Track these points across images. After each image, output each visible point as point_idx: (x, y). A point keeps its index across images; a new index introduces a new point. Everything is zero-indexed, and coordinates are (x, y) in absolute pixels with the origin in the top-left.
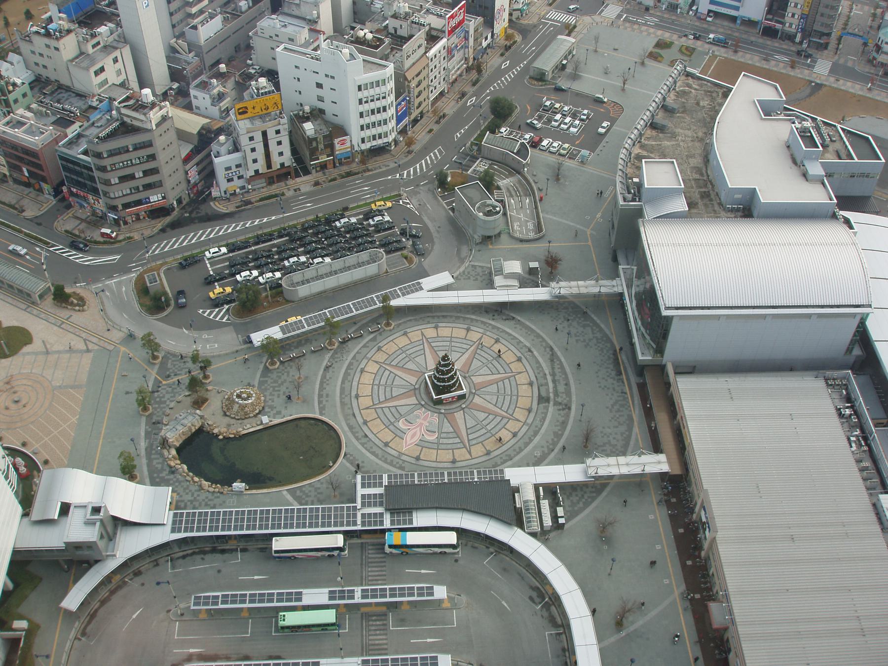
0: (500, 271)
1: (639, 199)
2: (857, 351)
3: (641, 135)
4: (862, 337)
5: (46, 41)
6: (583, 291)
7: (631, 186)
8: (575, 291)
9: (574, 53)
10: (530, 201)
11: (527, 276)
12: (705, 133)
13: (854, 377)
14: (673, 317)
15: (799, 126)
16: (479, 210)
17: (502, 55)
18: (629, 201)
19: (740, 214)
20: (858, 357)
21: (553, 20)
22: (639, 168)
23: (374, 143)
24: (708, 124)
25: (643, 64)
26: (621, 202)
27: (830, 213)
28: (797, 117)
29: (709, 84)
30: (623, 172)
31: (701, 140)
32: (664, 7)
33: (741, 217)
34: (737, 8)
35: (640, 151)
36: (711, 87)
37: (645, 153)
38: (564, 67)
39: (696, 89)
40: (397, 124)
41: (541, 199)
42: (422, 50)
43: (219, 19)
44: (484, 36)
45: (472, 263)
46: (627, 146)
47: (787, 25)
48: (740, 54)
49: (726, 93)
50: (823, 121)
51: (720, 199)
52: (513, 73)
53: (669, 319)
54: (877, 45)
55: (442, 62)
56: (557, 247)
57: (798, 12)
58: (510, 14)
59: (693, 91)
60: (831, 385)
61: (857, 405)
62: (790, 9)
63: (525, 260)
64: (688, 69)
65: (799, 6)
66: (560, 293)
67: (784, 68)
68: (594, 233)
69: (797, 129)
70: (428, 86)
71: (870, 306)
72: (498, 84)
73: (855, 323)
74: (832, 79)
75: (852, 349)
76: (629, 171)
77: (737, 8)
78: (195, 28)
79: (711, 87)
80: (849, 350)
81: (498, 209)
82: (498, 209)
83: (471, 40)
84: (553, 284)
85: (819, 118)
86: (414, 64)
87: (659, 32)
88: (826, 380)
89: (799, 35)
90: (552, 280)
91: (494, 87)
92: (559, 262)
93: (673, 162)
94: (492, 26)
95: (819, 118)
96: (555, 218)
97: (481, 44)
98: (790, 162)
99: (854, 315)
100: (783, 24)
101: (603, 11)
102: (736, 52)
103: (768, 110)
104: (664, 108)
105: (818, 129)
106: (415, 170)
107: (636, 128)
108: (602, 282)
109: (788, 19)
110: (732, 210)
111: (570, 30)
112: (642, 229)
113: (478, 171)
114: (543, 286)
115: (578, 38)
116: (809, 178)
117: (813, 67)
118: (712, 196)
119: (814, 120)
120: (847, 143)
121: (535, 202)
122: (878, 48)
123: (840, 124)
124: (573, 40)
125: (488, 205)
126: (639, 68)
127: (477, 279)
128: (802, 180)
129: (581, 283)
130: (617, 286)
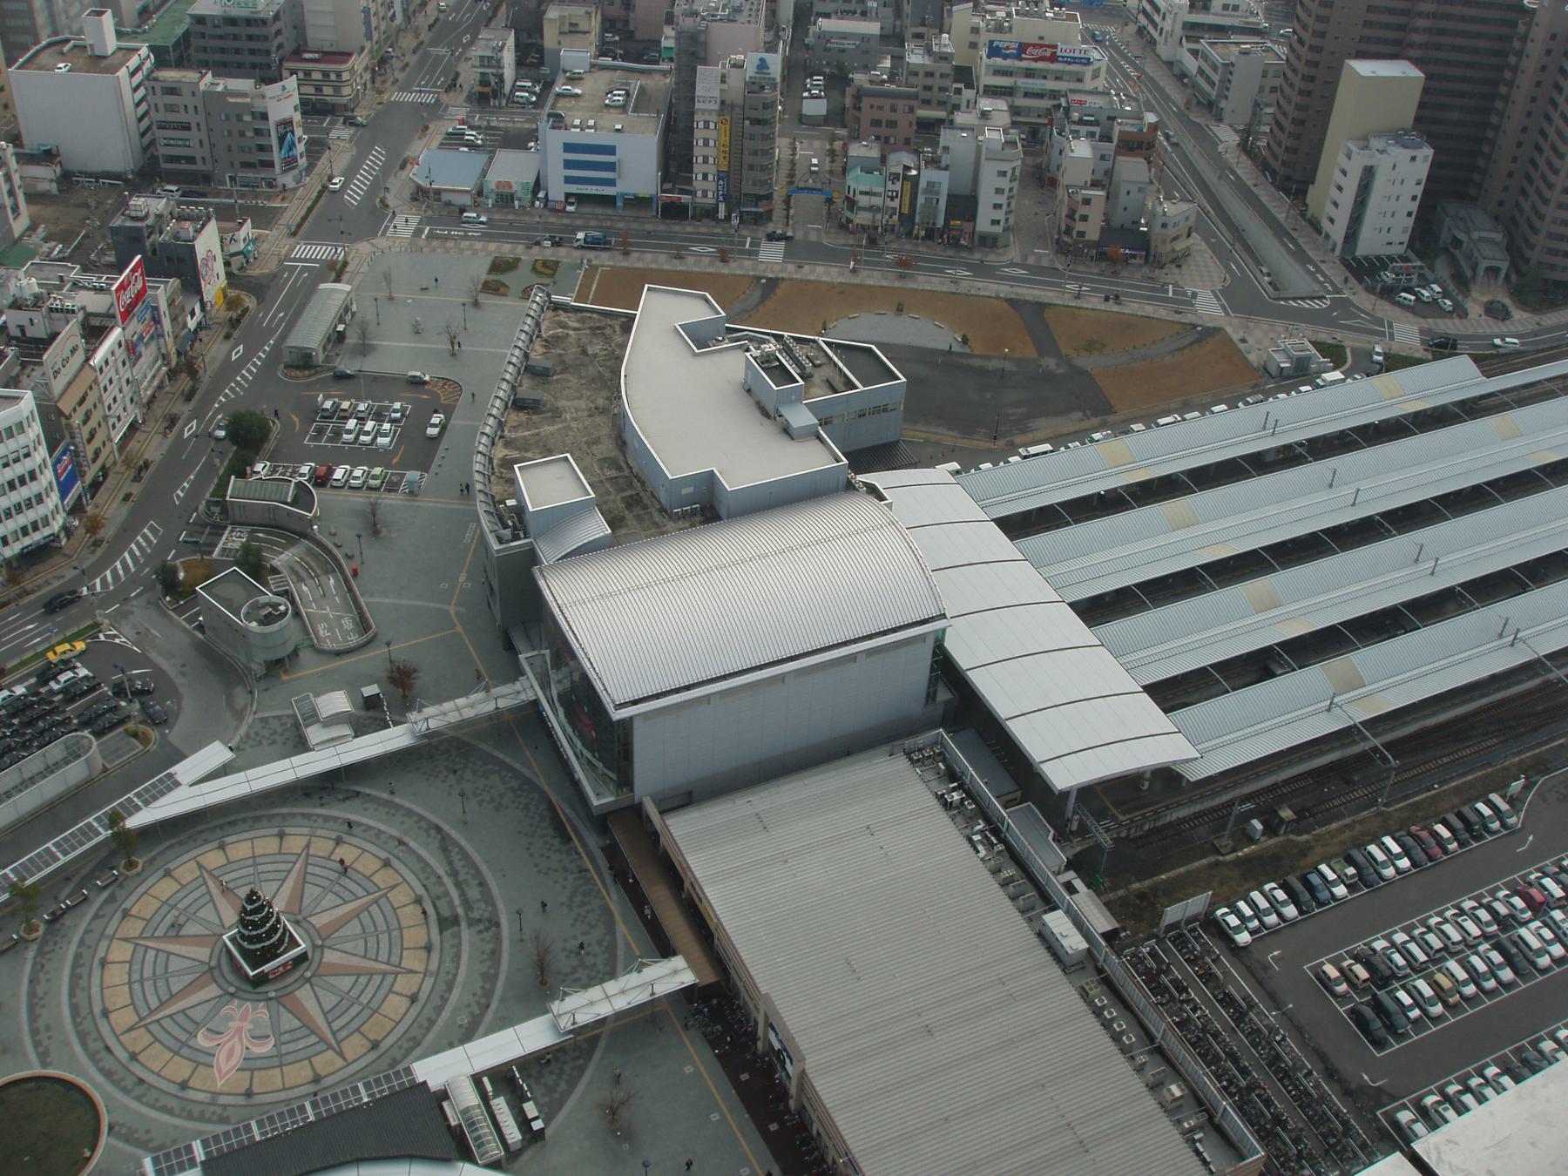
0: (313, 717)
1: (525, 534)
2: (944, 695)
3: (501, 425)
4: (945, 669)
6: (469, 713)
7: (506, 515)
8: (454, 718)
9: (354, 308)
10: (337, 580)
11: (363, 713)
12: (608, 398)
13: (951, 738)
14: (631, 718)
15: (757, 353)
16: (249, 617)
17: (227, 337)
18: (508, 542)
19: (698, 519)
20: (946, 703)
21: (305, 260)
22: (512, 481)
23: (27, 541)
24: (609, 382)
25: (476, 304)
26: (496, 546)
27: (842, 482)
28: (751, 339)
29: (595, 316)
30: (486, 494)
31: (604, 411)
32: (490, 202)
33: (702, 523)
34: (612, 183)
35: (506, 452)
37: (515, 454)
38: (341, 337)
39: (575, 329)
40: (63, 498)
41: (355, 573)
42: (80, 356)
44: (188, 310)
45: (260, 715)
46: (481, 448)
47: (699, 194)
48: (634, 256)
51: (660, 502)
52: (255, 365)
53: (627, 724)
54: (847, 198)
56: (403, 648)
57: (711, 170)
58: (227, 264)
59: (571, 332)
60: (918, 760)
61: (968, 781)
62: (698, 168)
63: (352, 687)
64: (554, 298)
65: (711, 160)
66: (428, 728)
67: (711, 264)
68: (462, 609)
69: (755, 359)
70: (106, 418)
71: (943, 616)
72: (232, 389)
73: (925, 654)
74: (791, 267)
75: (935, 692)
76: (496, 489)
77: (612, 183)
79: (600, 321)
80: (931, 696)
81: (282, 608)
82: (282, 608)
83: (166, 323)
84: (413, 716)
85: (786, 334)
86: (70, 383)
87: (492, 246)
88: (908, 754)
89: (722, 207)
90: (410, 709)
91: (226, 396)
92: (414, 675)
93: (566, 459)
94: (199, 292)
96: (387, 601)
97: (185, 325)
98: (758, 414)
99: (923, 637)
100: (692, 193)
102: (626, 253)
103: (701, 337)
104: (530, 370)
105: (788, 351)
106: (115, 573)
107: (490, 415)
108: (495, 691)
109: (698, 183)
110: (684, 516)
111: (337, 271)
112: (542, 583)
113: (231, 550)
114: (396, 724)
115: (356, 283)
116: (793, 433)
117: (757, 253)
118: (646, 501)
119: (778, 338)
121: (346, 581)
122: (851, 203)
124: (347, 288)
125: (264, 606)
127: (274, 742)
128: (785, 440)
129: (461, 701)
130: (526, 689)
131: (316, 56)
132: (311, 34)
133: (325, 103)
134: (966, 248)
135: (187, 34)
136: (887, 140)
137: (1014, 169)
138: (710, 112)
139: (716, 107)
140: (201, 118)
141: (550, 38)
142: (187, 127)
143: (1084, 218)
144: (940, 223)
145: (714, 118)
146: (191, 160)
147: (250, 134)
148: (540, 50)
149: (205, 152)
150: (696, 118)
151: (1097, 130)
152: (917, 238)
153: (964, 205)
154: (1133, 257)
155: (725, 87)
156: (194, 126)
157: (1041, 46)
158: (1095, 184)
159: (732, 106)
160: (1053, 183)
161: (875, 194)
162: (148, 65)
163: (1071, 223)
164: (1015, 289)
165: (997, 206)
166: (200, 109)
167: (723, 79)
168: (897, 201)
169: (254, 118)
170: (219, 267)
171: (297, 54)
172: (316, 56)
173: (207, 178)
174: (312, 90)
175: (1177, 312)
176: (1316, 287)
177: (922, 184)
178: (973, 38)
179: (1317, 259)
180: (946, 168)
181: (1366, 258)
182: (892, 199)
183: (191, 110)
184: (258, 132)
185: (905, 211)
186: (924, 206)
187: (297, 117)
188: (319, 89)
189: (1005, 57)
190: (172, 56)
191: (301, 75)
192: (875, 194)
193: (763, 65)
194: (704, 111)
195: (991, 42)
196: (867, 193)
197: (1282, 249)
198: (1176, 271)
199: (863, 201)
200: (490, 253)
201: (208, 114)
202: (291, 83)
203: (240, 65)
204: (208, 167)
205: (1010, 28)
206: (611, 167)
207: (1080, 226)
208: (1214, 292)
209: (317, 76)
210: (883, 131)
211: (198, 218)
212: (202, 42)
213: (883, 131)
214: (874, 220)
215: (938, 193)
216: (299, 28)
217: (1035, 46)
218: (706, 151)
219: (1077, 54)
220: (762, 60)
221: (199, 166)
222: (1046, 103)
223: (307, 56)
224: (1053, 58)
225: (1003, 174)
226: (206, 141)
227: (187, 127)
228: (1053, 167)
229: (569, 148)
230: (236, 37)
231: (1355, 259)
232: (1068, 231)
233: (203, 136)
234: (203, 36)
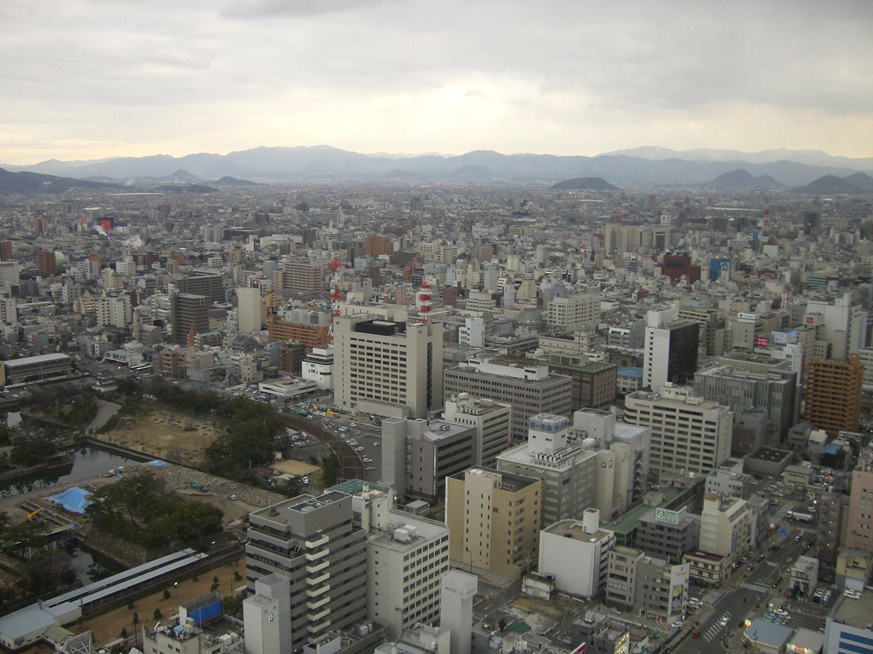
5: (170, 641)
43: (338, 640)
78: (313, 646)
131: (703, 554)
135: (636, 530)
140: (633, 576)
141: (841, 567)
142: (624, 579)
146: (623, 597)
147: (658, 590)
148: (833, 574)
149: (632, 595)
156: (629, 580)
162: (612, 542)
166: (634, 571)
171: (693, 551)
172: (703, 554)
173: (629, 609)
174: (697, 573)
183: (629, 570)
184: (663, 590)
187: (686, 586)
188: (700, 573)
190: (625, 540)
191: (692, 563)
202: (686, 566)
203: (660, 552)
204: (631, 603)
209: (701, 565)
211: (621, 630)
212: (643, 536)
216: (696, 537)
221: (627, 602)
223: (698, 553)
226: (633, 589)
227: (624, 579)
230: (661, 536)
234: (644, 532)
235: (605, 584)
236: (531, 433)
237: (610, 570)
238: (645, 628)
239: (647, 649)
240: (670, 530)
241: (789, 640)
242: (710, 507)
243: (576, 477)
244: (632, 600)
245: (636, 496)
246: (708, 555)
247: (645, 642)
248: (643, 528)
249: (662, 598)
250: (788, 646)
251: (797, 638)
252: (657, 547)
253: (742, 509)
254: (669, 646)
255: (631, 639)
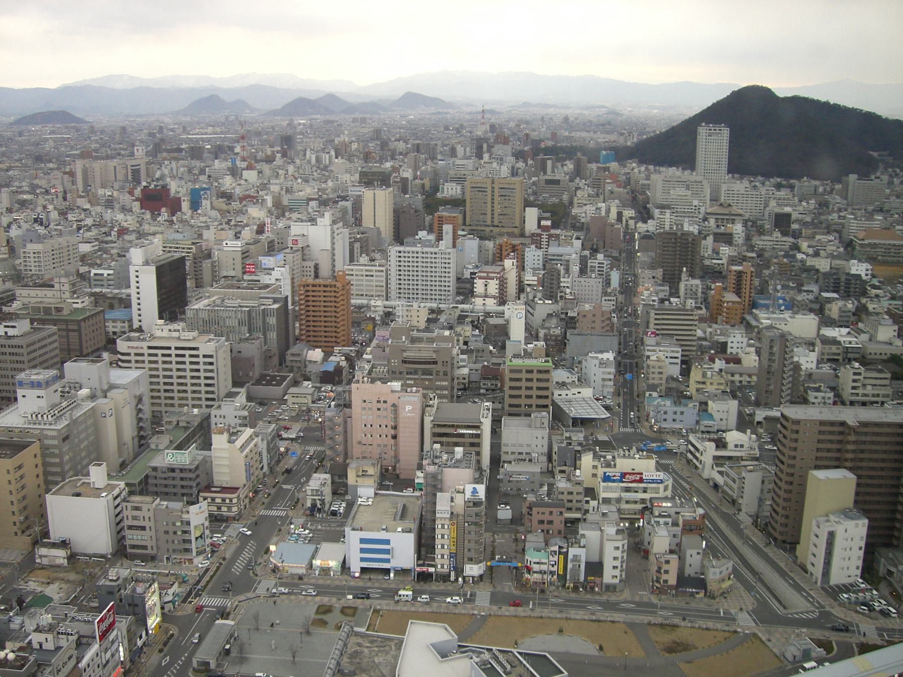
15: (477, 660)
17: (161, 651)
25: (308, 633)
28: (473, 652)
29: (379, 639)
32: (317, 573)
34: (388, 561)
36: (382, 642)
38: (228, 652)
39: (367, 647)
42: (73, 661)
47: (439, 566)
49: (399, 644)
50: (499, 650)
52: (175, 668)
54: (527, 567)
55: (97, 670)
57: (446, 552)
58: (162, 608)
59: (366, 650)
62: (438, 551)
64: (356, 629)
65: (446, 547)
69: (477, 663)
74: (495, 608)
77: (388, 561)
79: (382, 642)
89: (453, 574)
95: (494, 648)
97: (136, 644)
101: (256, 588)
103: (444, 653)
105: (496, 658)
109: (439, 561)
115: (237, 620)
117: (474, 601)
119: (489, 650)
120: (528, 666)
122: (529, 570)
123: (516, 648)
124: (232, 623)
126: (307, 639)
131: (219, 489)
132: (216, 478)
133: (222, 516)
134: (598, 593)
135: (147, 477)
136: (548, 531)
137: (623, 545)
138: (445, 519)
139: (449, 516)
140: (152, 524)
141: (351, 478)
142: (143, 528)
143: (666, 572)
144: (582, 578)
145: (447, 522)
146: (145, 548)
147: (179, 533)
148: (346, 485)
149: (154, 543)
150: (437, 522)
151: (669, 520)
152: (568, 588)
153: (595, 568)
154: (698, 593)
155: (453, 504)
156: (148, 528)
157: (634, 474)
158: (671, 552)
159: (458, 515)
160: (646, 553)
161: (542, 563)
162: (124, 493)
163: (659, 575)
164: (630, 616)
165: (615, 567)
166: (152, 519)
167: (452, 500)
168: (556, 567)
169: (182, 524)
170: (158, 609)
171: (208, 488)
172: (219, 489)
173: (153, 558)
174: (215, 509)
175: (728, 626)
176: (809, 605)
177: (570, 556)
178: (594, 471)
179: (807, 589)
180: (584, 547)
181: (837, 586)
182: (553, 566)
184: (185, 532)
185: (561, 572)
186: (571, 570)
187: (207, 524)
188: (219, 508)
189: (614, 481)
190: (138, 489)
191: (209, 500)
192: (542, 563)
193: (475, 491)
194: (441, 518)
195: (605, 473)
196: (538, 563)
197: (786, 584)
198: (724, 600)
199: (536, 567)
200: (316, 603)
201: (155, 522)
202: (204, 505)
203: (175, 494)
204: (155, 552)
205: (615, 465)
206: (387, 552)
207: (664, 577)
208: (748, 612)
209: (218, 501)
210: (545, 526)
211: (148, 581)
212: (154, 481)
213: (545, 526)
214: (543, 579)
215: (580, 561)
216: (209, 474)
217: (630, 474)
218: (443, 541)
219: (654, 478)
220: (474, 488)
221: (149, 551)
222: (639, 507)
223: (213, 489)
224: (641, 481)
225: (617, 548)
226: (154, 538)
227: (143, 528)
228: (646, 543)
229: (363, 541)
230: (174, 479)
231: (831, 587)
232: (658, 581)
233: (153, 533)
234: (156, 478)
235: (124, 537)
236: (20, 392)
237: (126, 523)
238: (174, 574)
239: (178, 595)
240: (181, 470)
241: (313, 557)
242: (219, 441)
243: (75, 432)
244: (155, 548)
245: (142, 442)
246: (224, 490)
247: (175, 588)
248: (154, 474)
249: (184, 541)
250: (314, 562)
251: (320, 553)
252: (172, 490)
253: (251, 438)
254: (199, 587)
255: (160, 588)
